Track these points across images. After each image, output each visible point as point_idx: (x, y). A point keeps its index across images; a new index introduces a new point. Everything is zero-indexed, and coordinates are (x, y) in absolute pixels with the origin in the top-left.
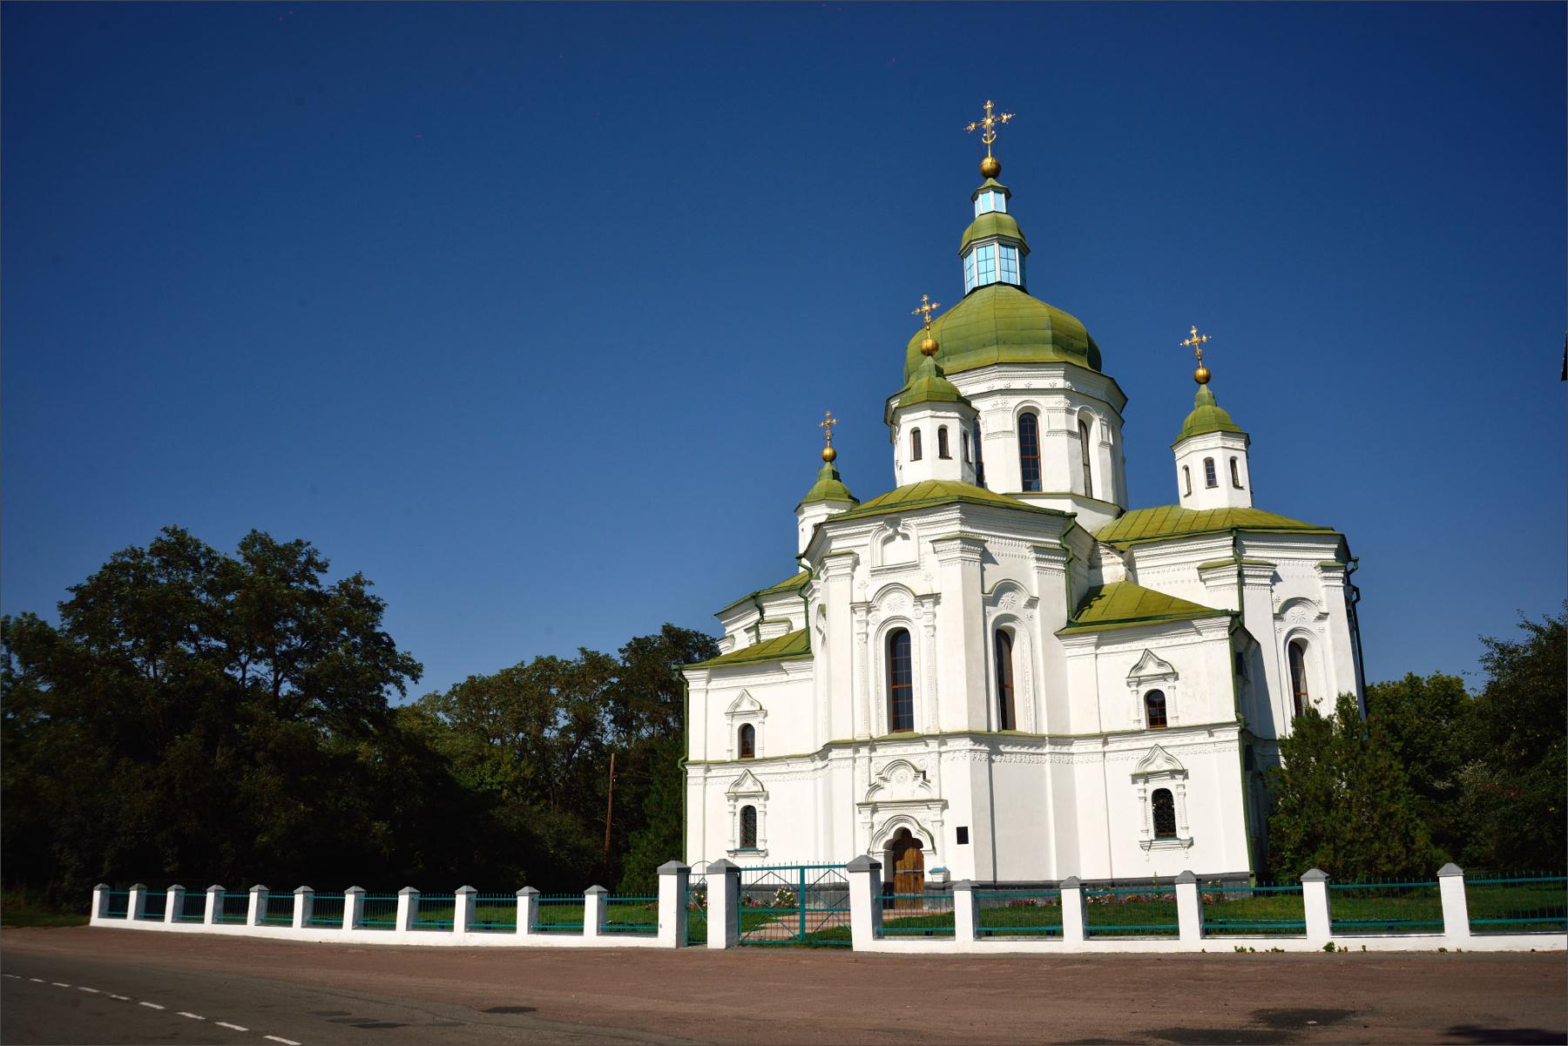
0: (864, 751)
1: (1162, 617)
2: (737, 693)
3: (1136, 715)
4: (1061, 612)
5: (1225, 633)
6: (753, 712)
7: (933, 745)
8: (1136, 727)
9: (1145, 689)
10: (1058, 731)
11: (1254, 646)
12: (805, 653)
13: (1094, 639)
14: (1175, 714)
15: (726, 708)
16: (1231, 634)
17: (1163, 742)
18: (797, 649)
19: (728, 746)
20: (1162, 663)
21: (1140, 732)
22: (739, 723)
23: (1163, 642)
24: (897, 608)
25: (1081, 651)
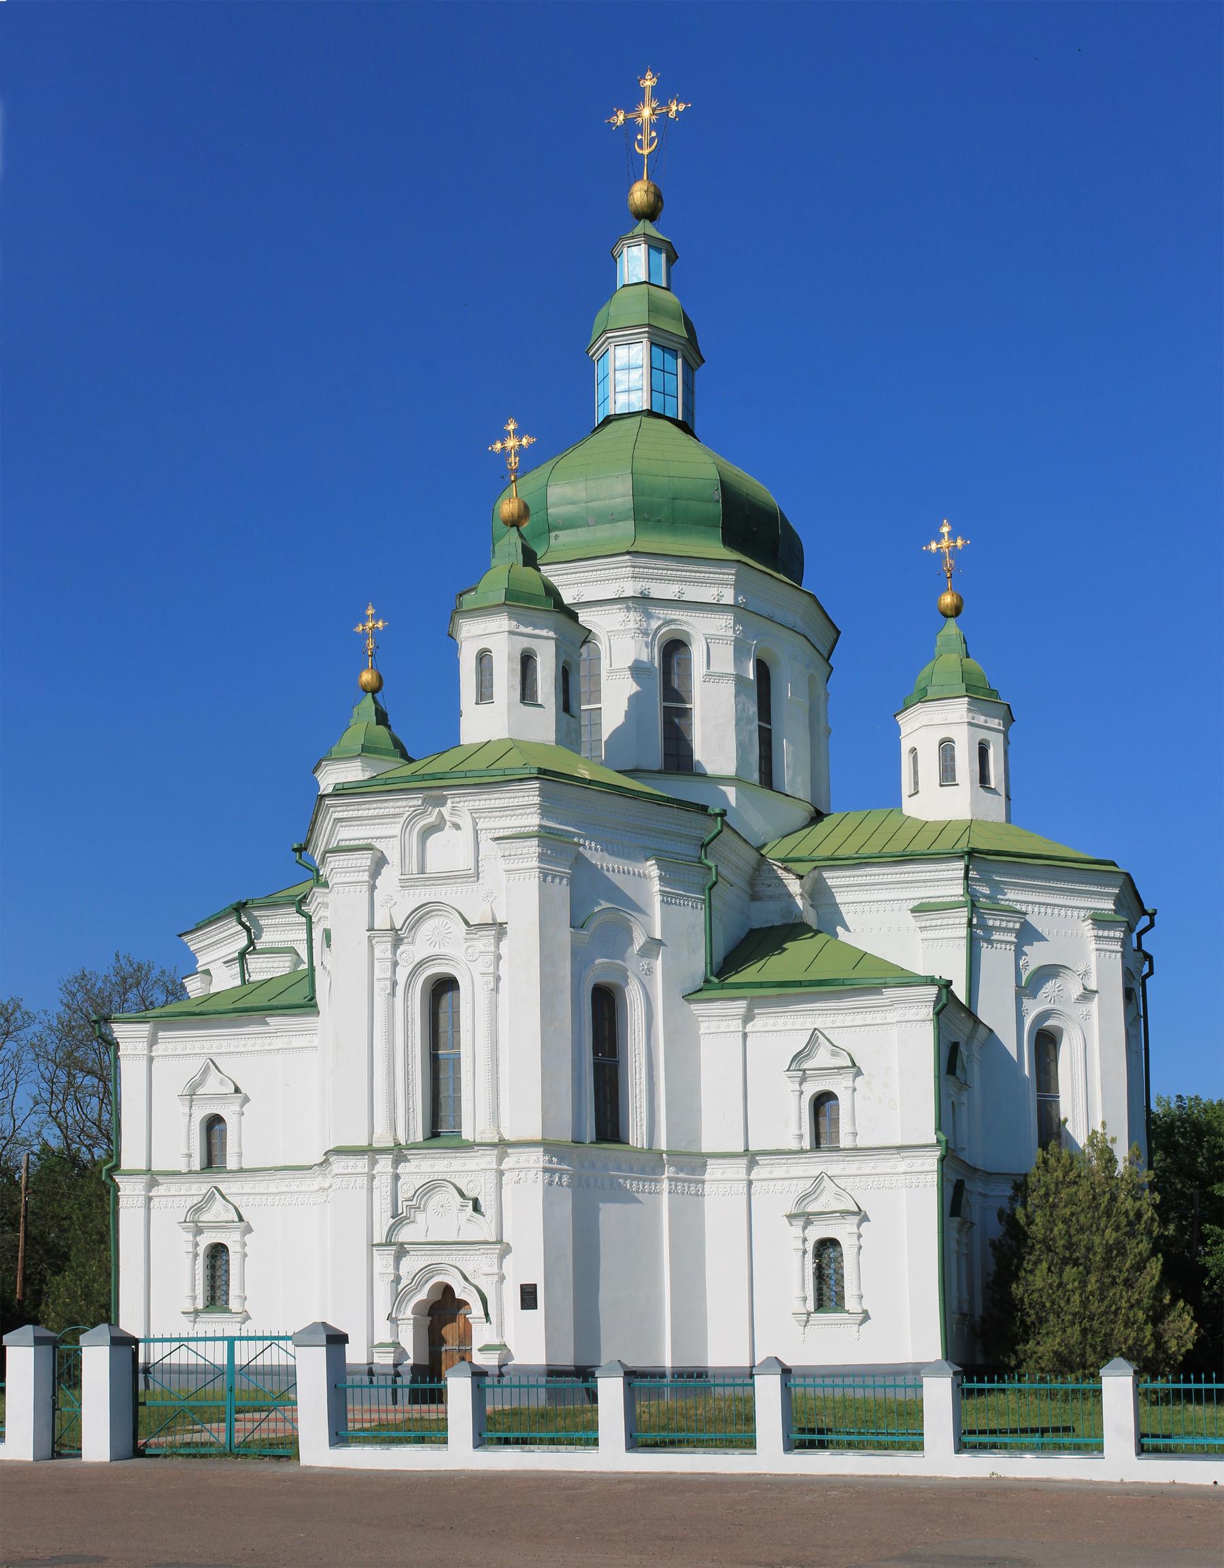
0: (384, 1164)
1: (842, 982)
2: (199, 1063)
3: (792, 1126)
4: (697, 965)
5: (928, 1012)
6: (222, 1097)
7: (487, 1160)
8: (794, 1145)
9: (812, 1088)
10: (681, 1148)
11: (982, 1033)
12: (309, 1005)
13: (740, 1006)
14: (850, 1124)
15: (181, 1086)
16: (938, 1014)
17: (833, 1169)
18: (296, 998)
19: (178, 1145)
20: (836, 1050)
21: (802, 1151)
22: (202, 1111)
23: (840, 1020)
24: (443, 945)
25: (723, 1026)
